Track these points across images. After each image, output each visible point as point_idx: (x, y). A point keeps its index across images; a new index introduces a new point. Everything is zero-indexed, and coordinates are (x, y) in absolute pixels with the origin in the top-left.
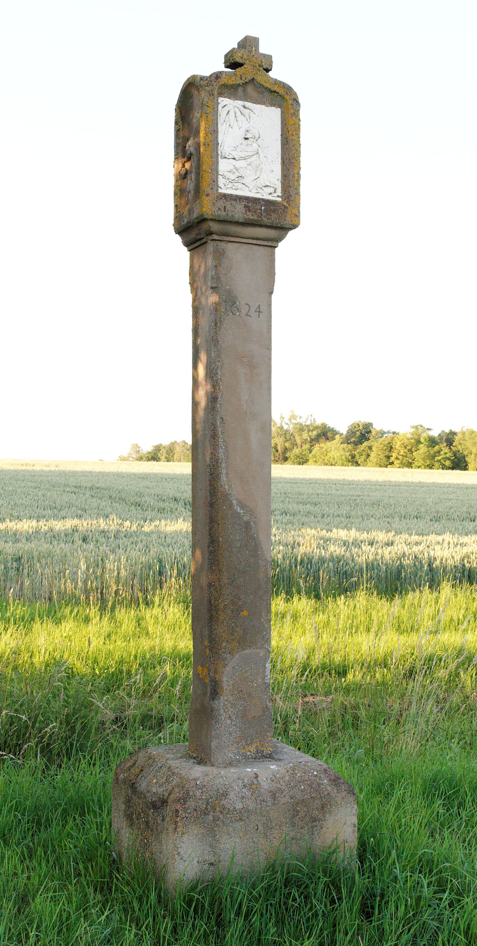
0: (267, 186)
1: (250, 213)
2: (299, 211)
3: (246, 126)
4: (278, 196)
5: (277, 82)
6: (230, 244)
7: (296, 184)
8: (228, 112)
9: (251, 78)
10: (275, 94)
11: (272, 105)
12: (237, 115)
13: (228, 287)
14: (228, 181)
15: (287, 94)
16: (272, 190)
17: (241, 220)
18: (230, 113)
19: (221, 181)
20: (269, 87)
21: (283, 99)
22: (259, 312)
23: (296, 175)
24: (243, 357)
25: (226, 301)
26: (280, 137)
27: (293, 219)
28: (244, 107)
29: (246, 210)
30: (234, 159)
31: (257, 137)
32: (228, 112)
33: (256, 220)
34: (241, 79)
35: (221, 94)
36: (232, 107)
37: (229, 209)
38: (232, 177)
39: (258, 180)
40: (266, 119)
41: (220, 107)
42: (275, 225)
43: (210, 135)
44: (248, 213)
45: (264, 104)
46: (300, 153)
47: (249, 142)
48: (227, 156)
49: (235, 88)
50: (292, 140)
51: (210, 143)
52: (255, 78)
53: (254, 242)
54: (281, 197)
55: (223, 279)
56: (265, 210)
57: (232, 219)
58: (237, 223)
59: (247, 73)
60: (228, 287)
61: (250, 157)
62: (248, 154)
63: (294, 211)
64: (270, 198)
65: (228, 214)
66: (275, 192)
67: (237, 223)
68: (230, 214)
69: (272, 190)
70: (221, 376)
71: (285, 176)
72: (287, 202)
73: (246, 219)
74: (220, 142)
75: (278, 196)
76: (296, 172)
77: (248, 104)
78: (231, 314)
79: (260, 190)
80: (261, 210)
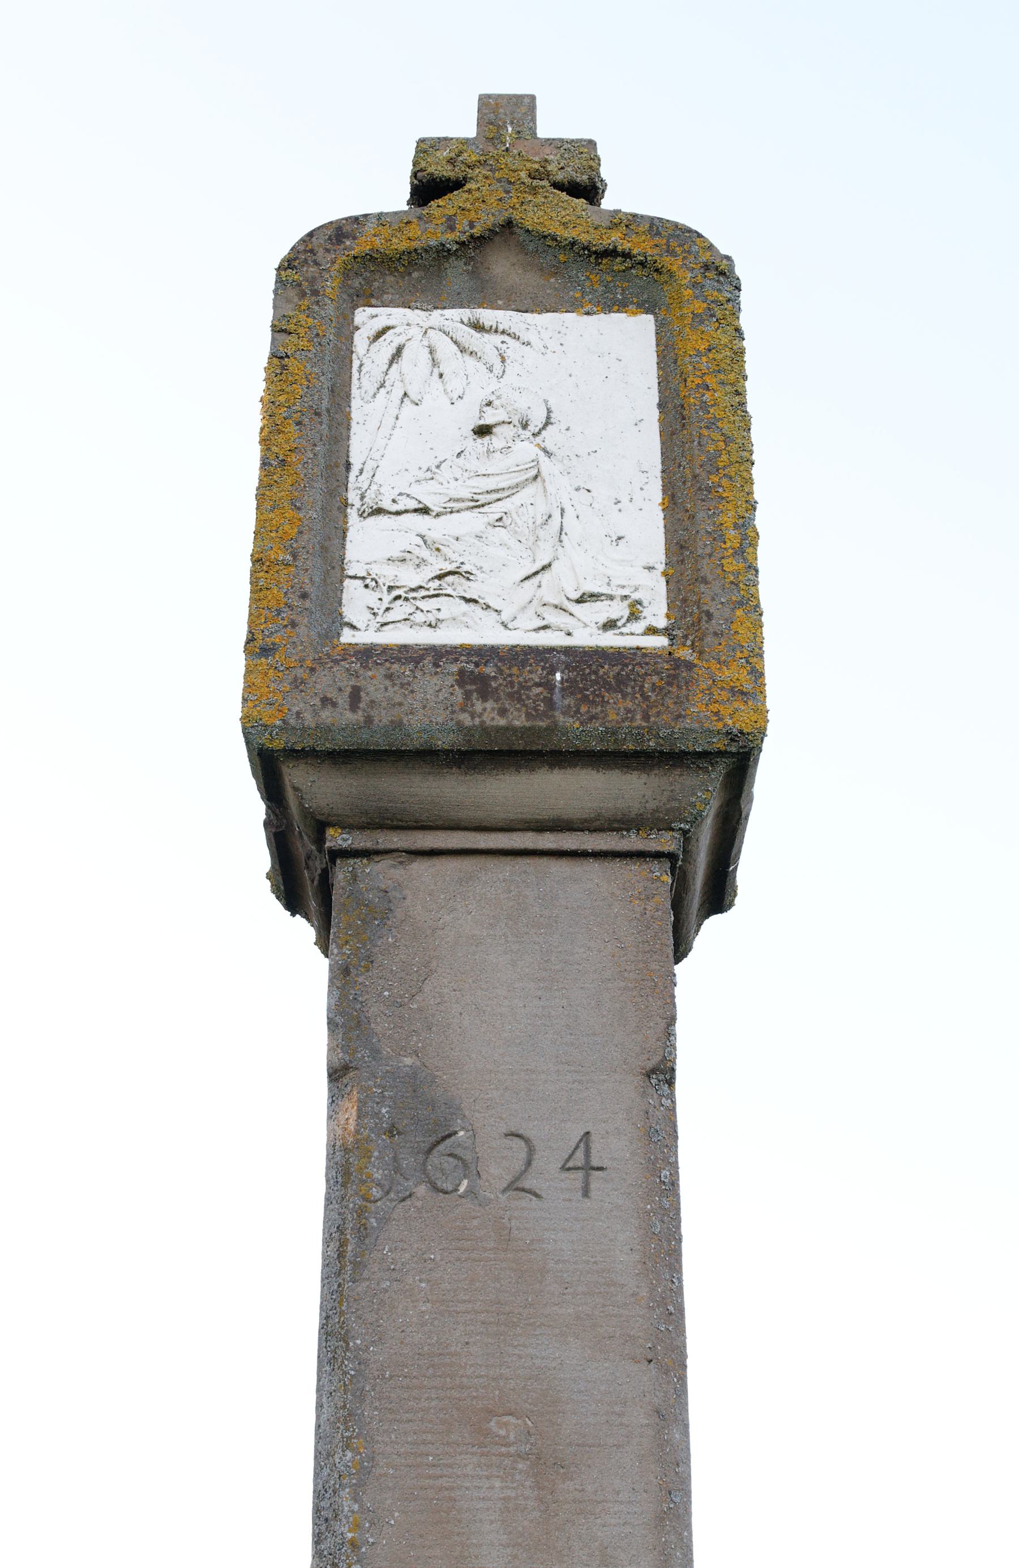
0: (594, 597)
1: (490, 705)
2: (758, 675)
3: (480, 384)
4: (652, 631)
5: (629, 222)
6: (420, 867)
7: (732, 565)
8: (399, 352)
9: (501, 219)
10: (618, 265)
11: (620, 306)
12: (439, 355)
13: (408, 1061)
14: (387, 598)
15: (671, 252)
16: (618, 610)
17: (443, 742)
18: (405, 353)
19: (356, 602)
20: (584, 238)
21: (668, 279)
22: (589, 1168)
23: (732, 533)
24: (491, 1413)
25: (392, 1131)
26: (656, 413)
27: (725, 711)
28: (478, 327)
29: (467, 695)
30: (425, 511)
31: (537, 419)
32: (399, 352)
33: (525, 731)
34: (452, 228)
35: (367, 297)
36: (415, 332)
37: (378, 696)
38: (409, 577)
39: (545, 577)
40: (597, 366)
41: (360, 341)
42: (630, 746)
43: (293, 428)
44: (479, 706)
45: (573, 306)
46: (746, 447)
47: (496, 441)
48: (387, 505)
49: (425, 268)
50: (704, 406)
51: (293, 458)
52: (516, 216)
53: (548, 841)
54: (667, 632)
55: (380, 1026)
56: (570, 687)
57: (399, 741)
58: (428, 757)
59: (502, 220)
60: (408, 1061)
61: (499, 494)
62: (491, 483)
63: (735, 674)
64: (610, 640)
65: (369, 720)
66: (634, 616)
67: (428, 757)
68: (382, 717)
69: (618, 610)
70: (357, 1526)
71: (680, 548)
72: (693, 646)
73: (469, 731)
74: (356, 458)
75: (652, 631)
76: (728, 519)
77: (488, 316)
78: (422, 1190)
79: (553, 617)
80: (549, 686)
